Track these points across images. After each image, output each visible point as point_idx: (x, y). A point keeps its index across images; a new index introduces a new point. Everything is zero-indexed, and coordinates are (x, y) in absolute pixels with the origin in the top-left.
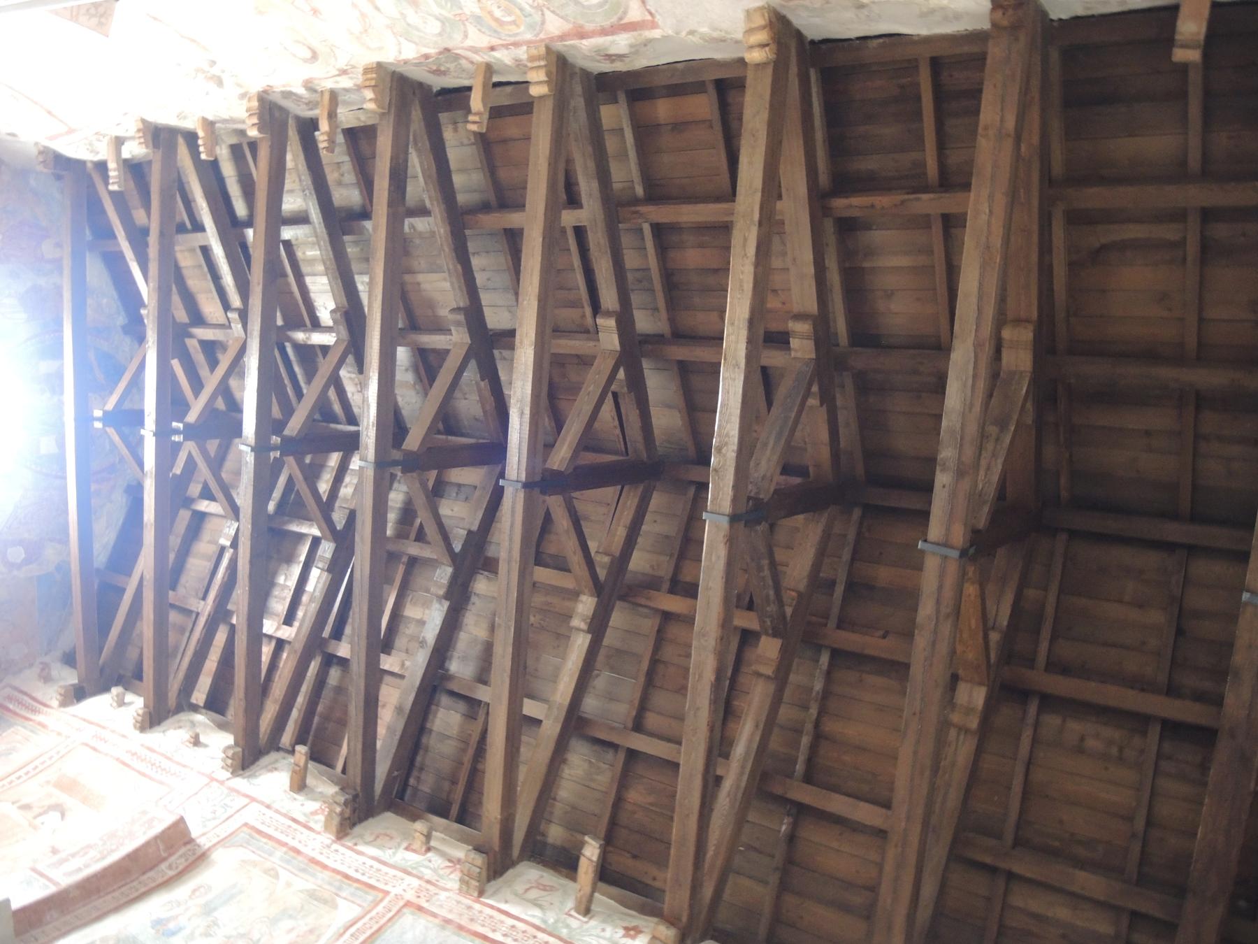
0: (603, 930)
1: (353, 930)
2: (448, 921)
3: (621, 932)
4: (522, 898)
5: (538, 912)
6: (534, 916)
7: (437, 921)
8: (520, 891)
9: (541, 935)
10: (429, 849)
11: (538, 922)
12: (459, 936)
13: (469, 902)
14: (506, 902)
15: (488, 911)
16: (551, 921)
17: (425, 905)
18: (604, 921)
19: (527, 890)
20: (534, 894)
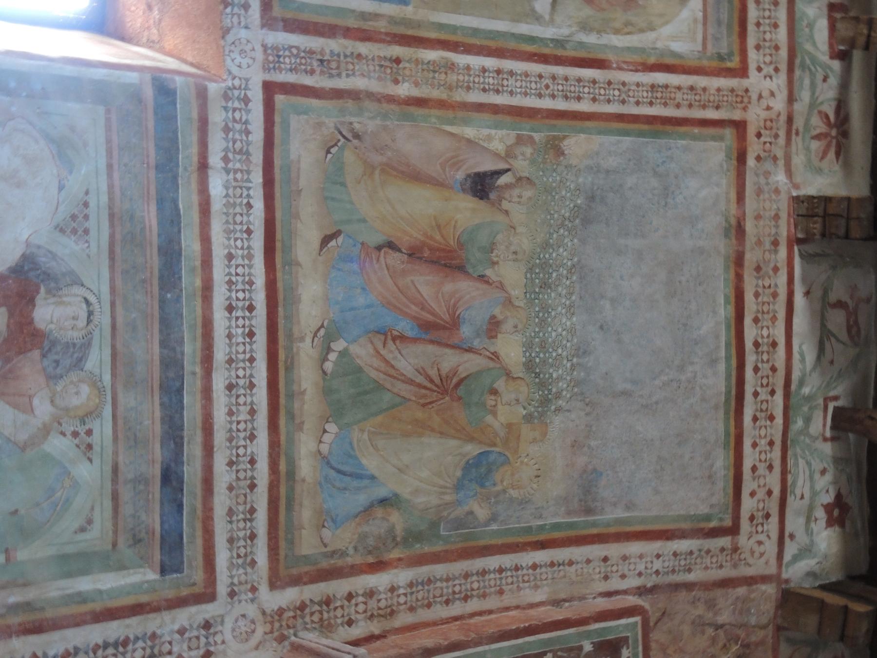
0: (823, 472)
1: (661, 78)
2: (740, 231)
3: (829, 498)
4: (824, 306)
5: (810, 357)
6: (803, 360)
7: (733, 209)
8: (833, 297)
9: (779, 398)
10: (844, 56)
11: (796, 375)
12: (727, 269)
13: (784, 232)
14: (807, 293)
15: (782, 279)
16: (806, 390)
17: (751, 162)
18: (837, 461)
19: (840, 304)
20: (837, 320)
